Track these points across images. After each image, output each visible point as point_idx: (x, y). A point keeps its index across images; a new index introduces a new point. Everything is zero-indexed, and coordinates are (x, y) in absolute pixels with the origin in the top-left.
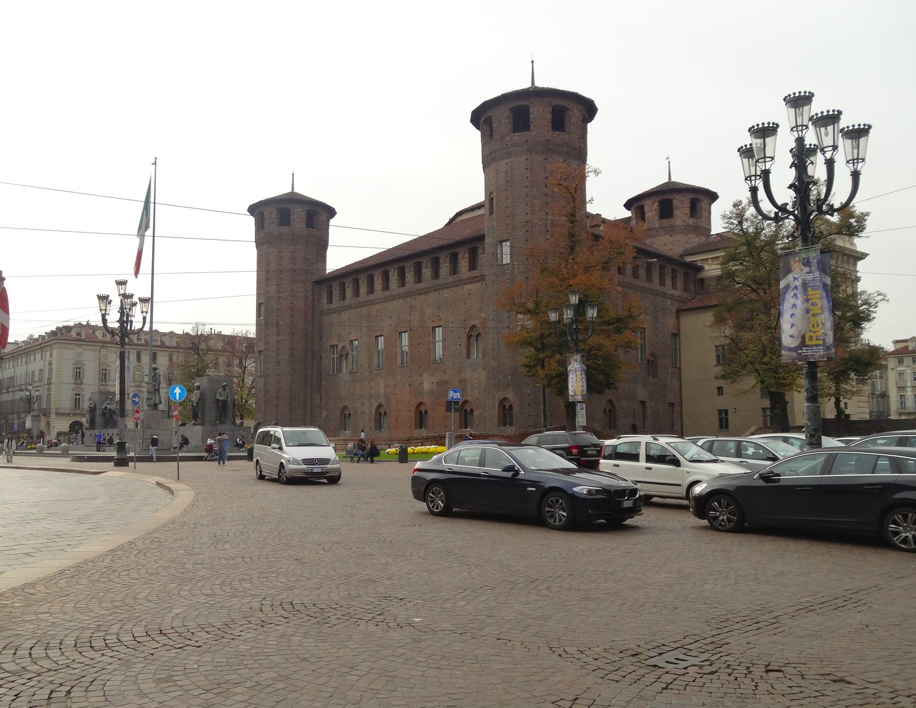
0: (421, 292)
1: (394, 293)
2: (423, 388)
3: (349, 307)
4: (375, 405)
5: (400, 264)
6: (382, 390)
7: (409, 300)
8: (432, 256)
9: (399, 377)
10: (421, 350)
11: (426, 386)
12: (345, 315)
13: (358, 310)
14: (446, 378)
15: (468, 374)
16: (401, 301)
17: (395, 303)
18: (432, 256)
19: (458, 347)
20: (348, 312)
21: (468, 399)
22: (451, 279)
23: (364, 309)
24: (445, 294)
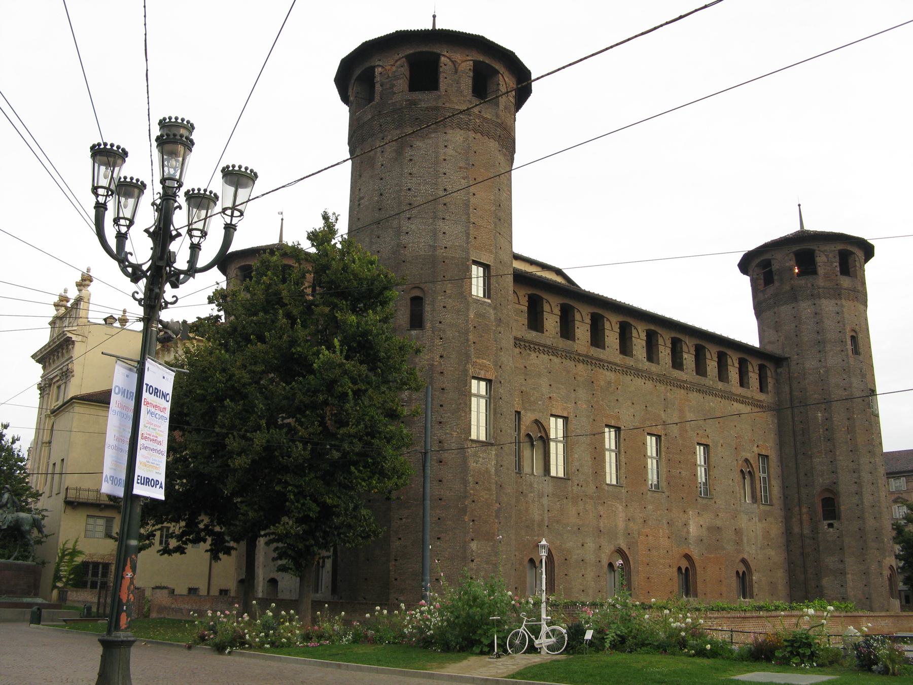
0: (681, 385)
1: (640, 366)
2: (688, 532)
3: (552, 350)
4: (608, 548)
5: (653, 328)
6: (621, 525)
7: (661, 388)
8: (699, 342)
9: (650, 507)
10: (684, 473)
11: (693, 529)
12: (537, 360)
13: (570, 364)
14: (719, 523)
15: (743, 522)
16: (649, 384)
17: (639, 382)
18: (699, 342)
19: (730, 481)
20: (546, 357)
21: (746, 556)
22: (720, 385)
23: (581, 367)
24: (713, 404)
